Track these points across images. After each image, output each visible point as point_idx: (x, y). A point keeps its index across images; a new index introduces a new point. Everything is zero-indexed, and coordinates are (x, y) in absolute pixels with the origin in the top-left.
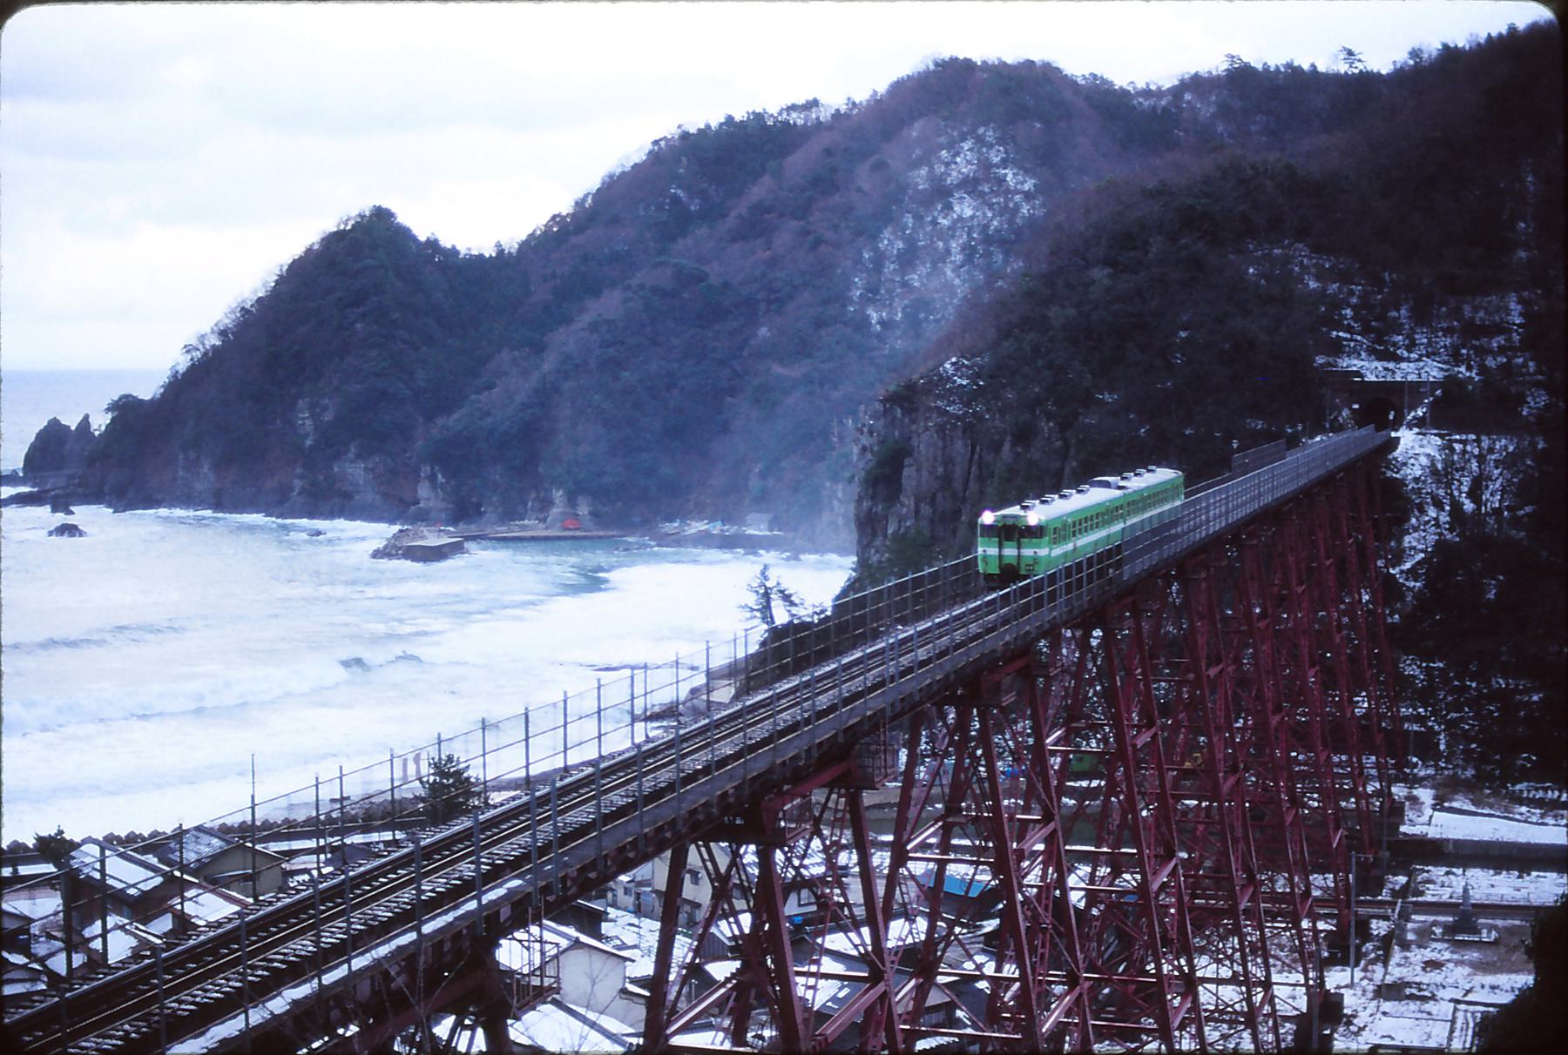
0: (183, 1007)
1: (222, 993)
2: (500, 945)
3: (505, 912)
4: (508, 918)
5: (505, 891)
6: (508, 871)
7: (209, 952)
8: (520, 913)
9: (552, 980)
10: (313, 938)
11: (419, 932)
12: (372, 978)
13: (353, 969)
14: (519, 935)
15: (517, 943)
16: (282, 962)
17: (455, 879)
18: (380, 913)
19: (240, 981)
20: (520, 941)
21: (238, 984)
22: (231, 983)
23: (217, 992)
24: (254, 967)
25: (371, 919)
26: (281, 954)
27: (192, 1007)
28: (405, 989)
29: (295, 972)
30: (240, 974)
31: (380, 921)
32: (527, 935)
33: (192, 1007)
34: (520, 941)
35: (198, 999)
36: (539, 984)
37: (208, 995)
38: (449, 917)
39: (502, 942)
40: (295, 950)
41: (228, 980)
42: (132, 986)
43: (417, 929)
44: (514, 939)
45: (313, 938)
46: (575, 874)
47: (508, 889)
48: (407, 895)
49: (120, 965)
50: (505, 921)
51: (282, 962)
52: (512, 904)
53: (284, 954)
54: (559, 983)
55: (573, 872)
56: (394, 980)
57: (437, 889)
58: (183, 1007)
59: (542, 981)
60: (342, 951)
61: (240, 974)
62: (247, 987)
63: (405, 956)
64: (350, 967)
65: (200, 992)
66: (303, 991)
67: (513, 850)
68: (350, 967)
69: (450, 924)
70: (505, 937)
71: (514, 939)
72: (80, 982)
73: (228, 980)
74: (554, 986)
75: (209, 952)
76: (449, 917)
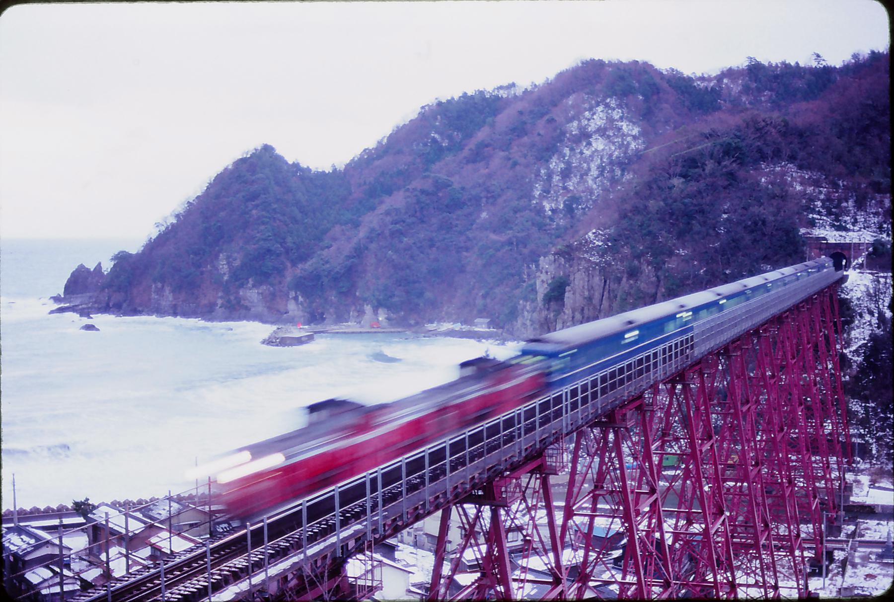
0: (173, 596)
1: (196, 588)
2: (348, 562)
3: (351, 544)
4: (353, 548)
5: (353, 532)
6: (353, 520)
7: (185, 566)
8: (360, 545)
9: (379, 582)
10: (247, 558)
11: (305, 554)
12: (278, 581)
13: (269, 575)
14: (360, 556)
15: (359, 562)
16: (228, 571)
17: (324, 524)
18: (282, 544)
19: (207, 582)
20: (360, 560)
21: (206, 584)
22: (200, 583)
23: (192, 588)
24: (213, 574)
25: (278, 547)
26: (228, 567)
27: (180, 597)
28: (315, 579)
29: (236, 576)
30: (205, 578)
31: (281, 548)
32: (364, 556)
33: (180, 597)
34: (360, 560)
35: (182, 592)
36: (371, 585)
37: (187, 589)
38: (322, 546)
39: (349, 560)
40: (235, 564)
41: (199, 581)
42: (144, 584)
43: (304, 552)
44: (357, 559)
45: (247, 558)
46: (390, 522)
47: (355, 531)
48: (298, 534)
49: (137, 573)
50: (351, 549)
51: (228, 571)
52: (356, 539)
53: (230, 567)
54: (382, 584)
55: (389, 522)
56: (289, 582)
57: (314, 530)
58: (173, 596)
59: (372, 583)
60: (259, 565)
61: (205, 578)
62: (210, 585)
63: (297, 569)
64: (267, 574)
65: (183, 588)
66: (243, 586)
67: (356, 508)
68: (267, 574)
69: (321, 550)
70: (351, 558)
71: (357, 559)
72: (115, 582)
73: (199, 581)
74: (380, 585)
75: (185, 566)
76: (322, 546)
